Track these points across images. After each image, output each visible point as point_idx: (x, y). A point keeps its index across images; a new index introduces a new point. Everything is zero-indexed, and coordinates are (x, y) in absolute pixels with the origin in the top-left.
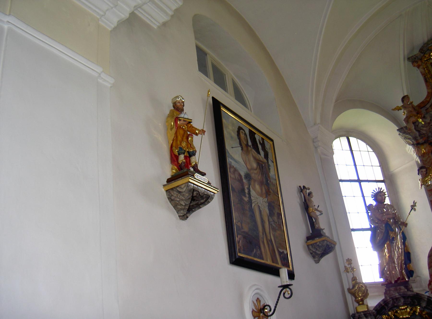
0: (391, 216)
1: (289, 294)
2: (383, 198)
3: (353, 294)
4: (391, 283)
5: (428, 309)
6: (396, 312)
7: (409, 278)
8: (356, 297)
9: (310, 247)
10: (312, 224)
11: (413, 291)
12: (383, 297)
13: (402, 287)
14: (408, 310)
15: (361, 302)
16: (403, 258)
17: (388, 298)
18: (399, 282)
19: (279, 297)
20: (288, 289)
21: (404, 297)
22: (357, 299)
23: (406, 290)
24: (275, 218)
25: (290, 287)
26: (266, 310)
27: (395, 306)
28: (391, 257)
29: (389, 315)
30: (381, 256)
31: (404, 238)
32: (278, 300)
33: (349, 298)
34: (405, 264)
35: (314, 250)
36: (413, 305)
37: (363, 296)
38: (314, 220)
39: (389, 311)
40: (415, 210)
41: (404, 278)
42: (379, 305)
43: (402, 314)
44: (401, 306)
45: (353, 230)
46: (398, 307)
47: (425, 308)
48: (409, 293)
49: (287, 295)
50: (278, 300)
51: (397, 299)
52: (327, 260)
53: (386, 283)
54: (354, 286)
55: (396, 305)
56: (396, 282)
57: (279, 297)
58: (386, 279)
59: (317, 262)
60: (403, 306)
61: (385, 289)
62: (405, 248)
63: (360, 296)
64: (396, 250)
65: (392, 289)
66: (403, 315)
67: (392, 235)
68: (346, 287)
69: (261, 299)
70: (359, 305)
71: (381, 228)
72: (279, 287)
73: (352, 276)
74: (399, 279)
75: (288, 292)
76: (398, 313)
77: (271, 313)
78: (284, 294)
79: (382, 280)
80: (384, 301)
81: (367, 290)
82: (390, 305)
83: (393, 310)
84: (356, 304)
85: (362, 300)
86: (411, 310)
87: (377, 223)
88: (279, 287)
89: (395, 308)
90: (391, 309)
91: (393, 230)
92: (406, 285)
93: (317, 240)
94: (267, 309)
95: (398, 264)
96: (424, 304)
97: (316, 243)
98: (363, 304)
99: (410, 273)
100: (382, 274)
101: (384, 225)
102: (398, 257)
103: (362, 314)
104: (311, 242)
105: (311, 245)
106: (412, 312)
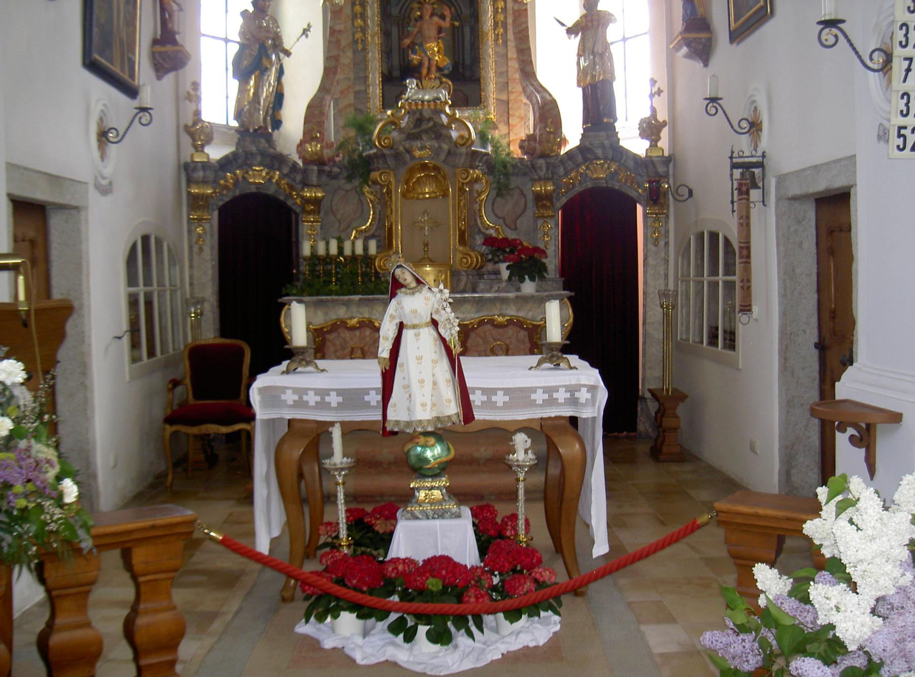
0: (271, 35)
1: (147, 120)
2: (266, 5)
3: (192, 135)
4: (248, 130)
5: (289, 177)
6: (247, 172)
7: (273, 130)
8: (194, 140)
9: (157, 55)
10: (164, 23)
11: (275, 149)
12: (233, 149)
13: (263, 141)
14: (264, 174)
15: (199, 149)
16: (272, 99)
17: (241, 151)
18: (259, 132)
19: (132, 121)
20: (147, 114)
21: (263, 154)
22: (196, 143)
23: (267, 145)
24: (131, 7)
25: (150, 111)
26: (111, 135)
27: (246, 164)
28: (257, 94)
29: (235, 174)
30: (242, 90)
31: (281, 72)
32: (131, 124)
33: (186, 140)
34: (273, 108)
35: (161, 61)
36: (271, 168)
37: (206, 141)
38: (167, 16)
39: (237, 168)
40: (307, 36)
41: (266, 128)
42: (226, 158)
43: (254, 176)
44: (256, 166)
45: (204, 35)
46: (250, 166)
47: (287, 175)
48: (271, 150)
49: (144, 121)
50: (131, 124)
51: (252, 154)
52: (169, 78)
53: (242, 129)
54: (195, 124)
55: (249, 162)
56: (255, 130)
57: (132, 121)
58: (242, 124)
59: (159, 78)
60: (259, 165)
61: (239, 139)
62: (279, 87)
63: (201, 140)
64: (266, 85)
65: (248, 139)
66: (254, 178)
67: (265, 62)
68: (182, 123)
69: (104, 119)
70: (197, 151)
71: (253, 48)
72: (136, 108)
73: (195, 108)
74: (260, 127)
75: (146, 118)
76: (249, 175)
77: (116, 140)
78: (140, 118)
79: (234, 124)
80: (233, 154)
81: (212, 133)
82: (240, 161)
83: (242, 169)
84: (192, 150)
85: (203, 146)
86: (267, 174)
87: (248, 39)
88: (136, 108)
89: (246, 167)
90: (240, 167)
91: (269, 58)
92: (269, 138)
93: (169, 48)
94: (112, 133)
95: (264, 107)
96: (286, 170)
97: (166, 52)
98: (203, 151)
99: (277, 123)
100: (238, 116)
101: (257, 46)
102: (267, 96)
103: (200, 164)
104: (158, 48)
105: (160, 53)
106: (268, 177)
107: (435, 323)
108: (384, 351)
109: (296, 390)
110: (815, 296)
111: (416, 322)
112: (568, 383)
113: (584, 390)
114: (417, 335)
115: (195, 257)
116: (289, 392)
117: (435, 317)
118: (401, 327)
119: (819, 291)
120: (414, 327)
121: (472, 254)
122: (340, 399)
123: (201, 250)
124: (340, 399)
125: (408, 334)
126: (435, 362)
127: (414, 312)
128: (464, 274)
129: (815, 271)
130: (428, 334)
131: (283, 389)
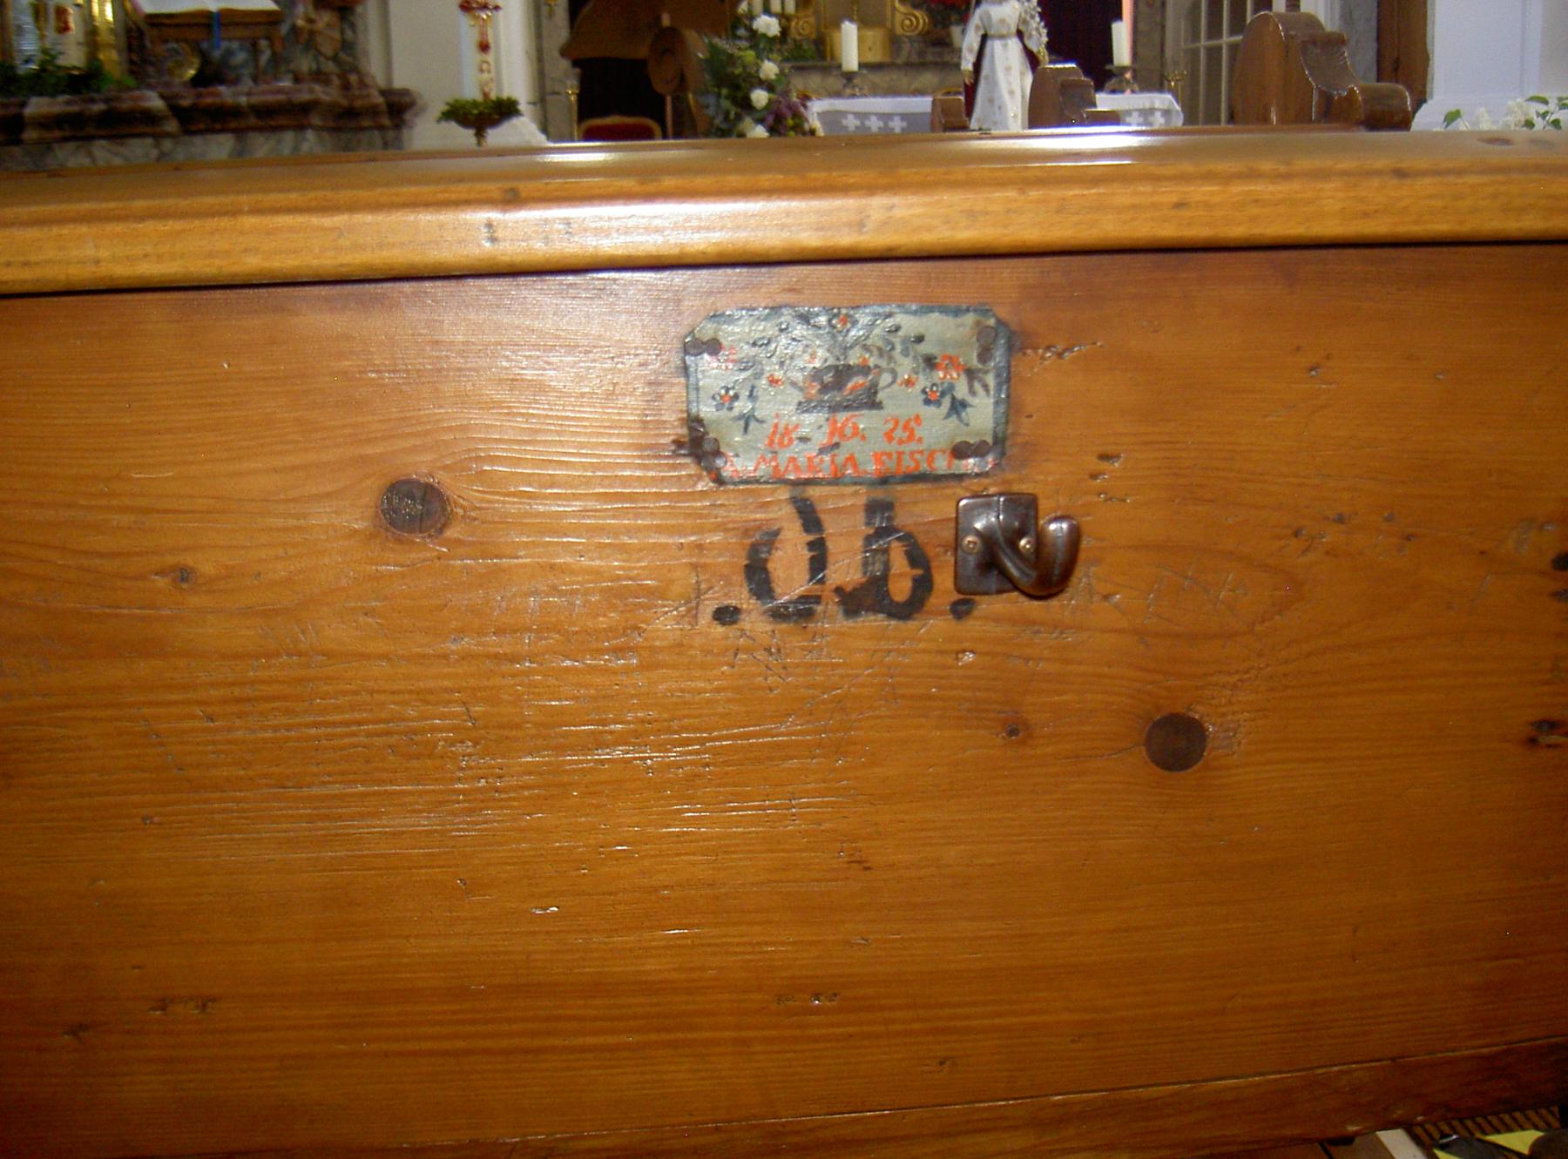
107: (1020, 34)
108: (967, 64)
109: (857, 115)
110: (1375, 45)
111: (1004, 32)
112: (1141, 107)
113: (1158, 114)
114: (1005, 46)
115: (545, 22)
116: (850, 117)
117: (1021, 28)
118: (984, 38)
119: (1379, 39)
120: (1002, 37)
121: (918, 13)
122: (904, 124)
123: (551, 14)
124: (904, 124)
125: (995, 46)
126: (1022, 74)
127: (1002, 21)
128: (906, 40)
129: (1375, 15)
130: (1014, 45)
131: (843, 114)
